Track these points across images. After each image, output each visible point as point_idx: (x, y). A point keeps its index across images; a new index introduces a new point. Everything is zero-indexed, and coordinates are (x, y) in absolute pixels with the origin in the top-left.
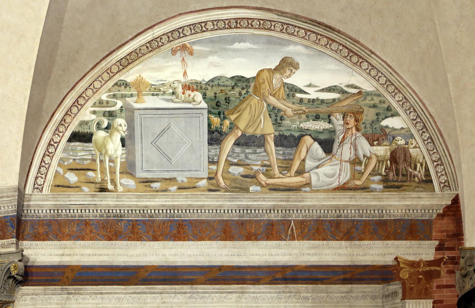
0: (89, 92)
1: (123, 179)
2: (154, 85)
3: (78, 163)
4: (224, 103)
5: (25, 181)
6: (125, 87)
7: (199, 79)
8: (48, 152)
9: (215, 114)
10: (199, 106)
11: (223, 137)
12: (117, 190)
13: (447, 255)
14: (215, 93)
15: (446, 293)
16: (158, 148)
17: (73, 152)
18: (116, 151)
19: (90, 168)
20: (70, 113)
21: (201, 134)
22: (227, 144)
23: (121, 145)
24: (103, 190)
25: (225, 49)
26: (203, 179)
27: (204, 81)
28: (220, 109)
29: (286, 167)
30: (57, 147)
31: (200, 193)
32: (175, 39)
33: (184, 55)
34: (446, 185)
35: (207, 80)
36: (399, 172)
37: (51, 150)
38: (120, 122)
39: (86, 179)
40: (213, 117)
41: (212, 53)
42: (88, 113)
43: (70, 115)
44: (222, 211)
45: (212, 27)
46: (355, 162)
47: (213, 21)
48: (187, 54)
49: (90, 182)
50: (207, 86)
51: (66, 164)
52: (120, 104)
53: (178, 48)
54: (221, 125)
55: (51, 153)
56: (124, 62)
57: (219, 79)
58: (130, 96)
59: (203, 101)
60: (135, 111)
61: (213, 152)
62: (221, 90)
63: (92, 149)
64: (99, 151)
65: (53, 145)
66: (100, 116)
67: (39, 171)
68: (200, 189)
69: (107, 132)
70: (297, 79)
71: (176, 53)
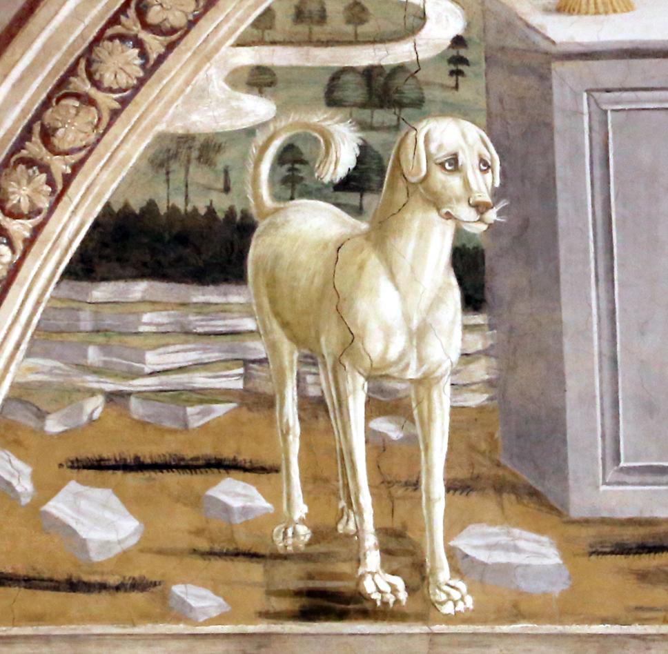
1: (474, 529)
3: (143, 424)
12: (433, 605)
19: (227, 453)
20: (87, 88)
23: (455, 295)
24: (328, 602)
39: (199, 532)
42: (218, 86)
49: (234, 550)
51: (53, 426)
63: (249, 324)
64: (295, 339)
66: (309, 105)
69: (358, 212)
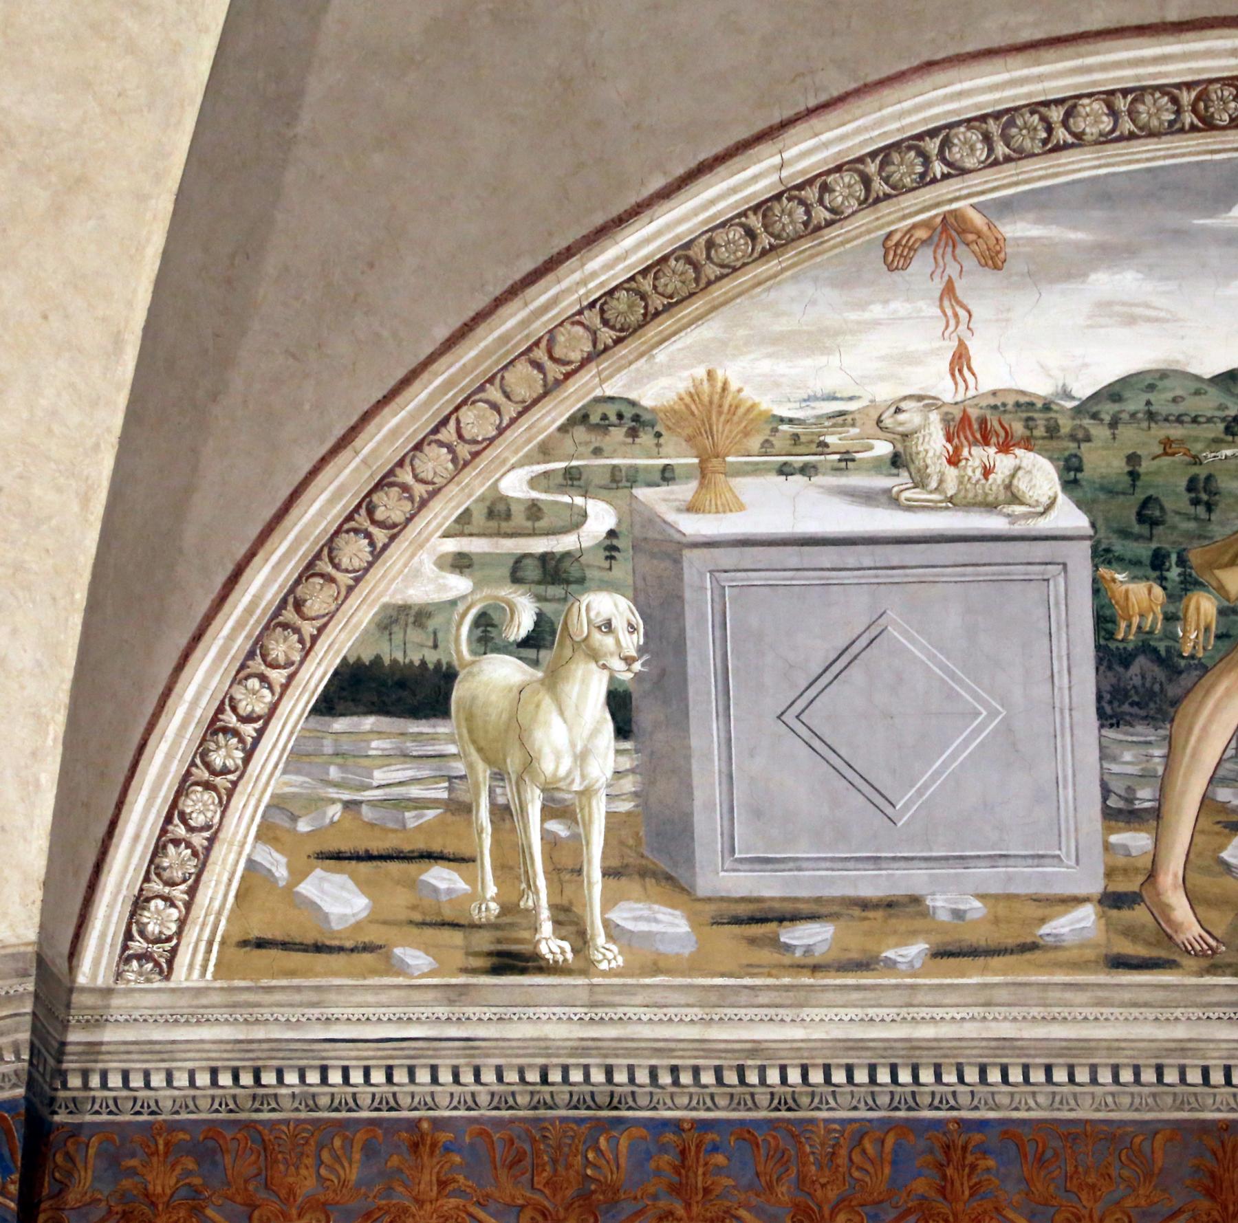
0: (435, 462)
1: (624, 905)
2: (791, 421)
3: (372, 825)
4: (1183, 503)
5: (74, 920)
6: (633, 433)
7: (1041, 387)
8: (207, 765)
9: (1136, 563)
10: (1043, 525)
11: (1185, 680)
12: (593, 963)
14: (1133, 459)
16: (816, 744)
17: (341, 766)
18: (582, 758)
19: (436, 847)
20: (329, 569)
21: (1060, 666)
22: (1210, 720)
23: (609, 727)
24: (512, 961)
25: (1180, 235)
26: (1078, 901)
27: (1068, 395)
28: (1164, 539)
30: (257, 741)
31: (1060, 978)
32: (900, 190)
33: (952, 270)
35: (1083, 389)
37: (225, 754)
38: (607, 607)
39: (414, 908)
40: (1119, 577)
41: (1108, 254)
42: (429, 568)
43: (331, 580)
44: (1194, 1077)
45: (1106, 124)
47: (1112, 93)
48: (970, 263)
49: (440, 922)
50: (1087, 422)
51: (303, 826)
52: (601, 518)
53: (922, 234)
54: (1170, 618)
55: (225, 771)
56: (623, 307)
57: (1151, 387)
58: (657, 477)
59: (1062, 498)
60: (687, 553)
61: (1128, 761)
62: (1167, 443)
63: (452, 749)
64: (487, 760)
65: (235, 733)
66: (498, 582)
67: (154, 868)
68: (1062, 956)
69: (535, 663)
71: (908, 260)
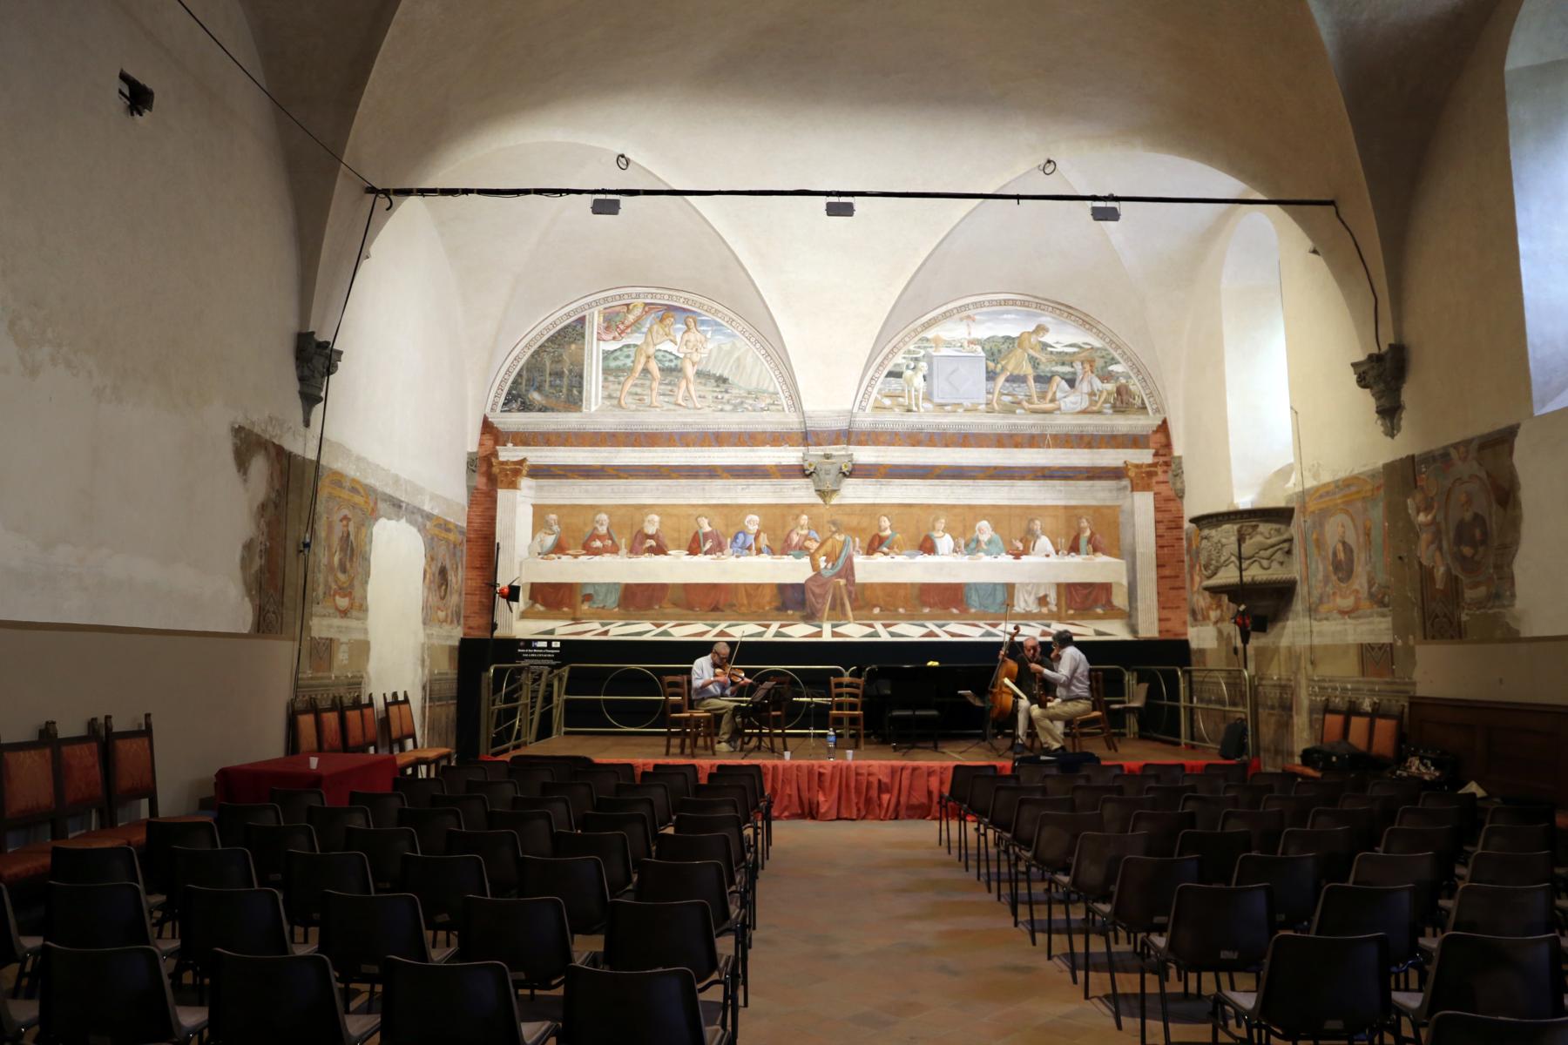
13: (1161, 459)
15: (1162, 488)
29: (1042, 396)
34: (1157, 411)
36: (1123, 401)
38: (923, 365)
46: (1092, 394)
52: (923, 352)
70: (1048, 338)
